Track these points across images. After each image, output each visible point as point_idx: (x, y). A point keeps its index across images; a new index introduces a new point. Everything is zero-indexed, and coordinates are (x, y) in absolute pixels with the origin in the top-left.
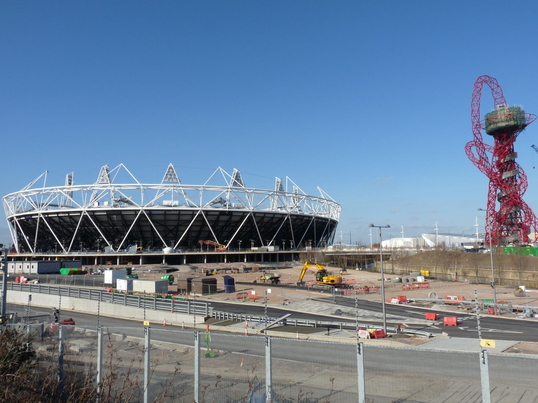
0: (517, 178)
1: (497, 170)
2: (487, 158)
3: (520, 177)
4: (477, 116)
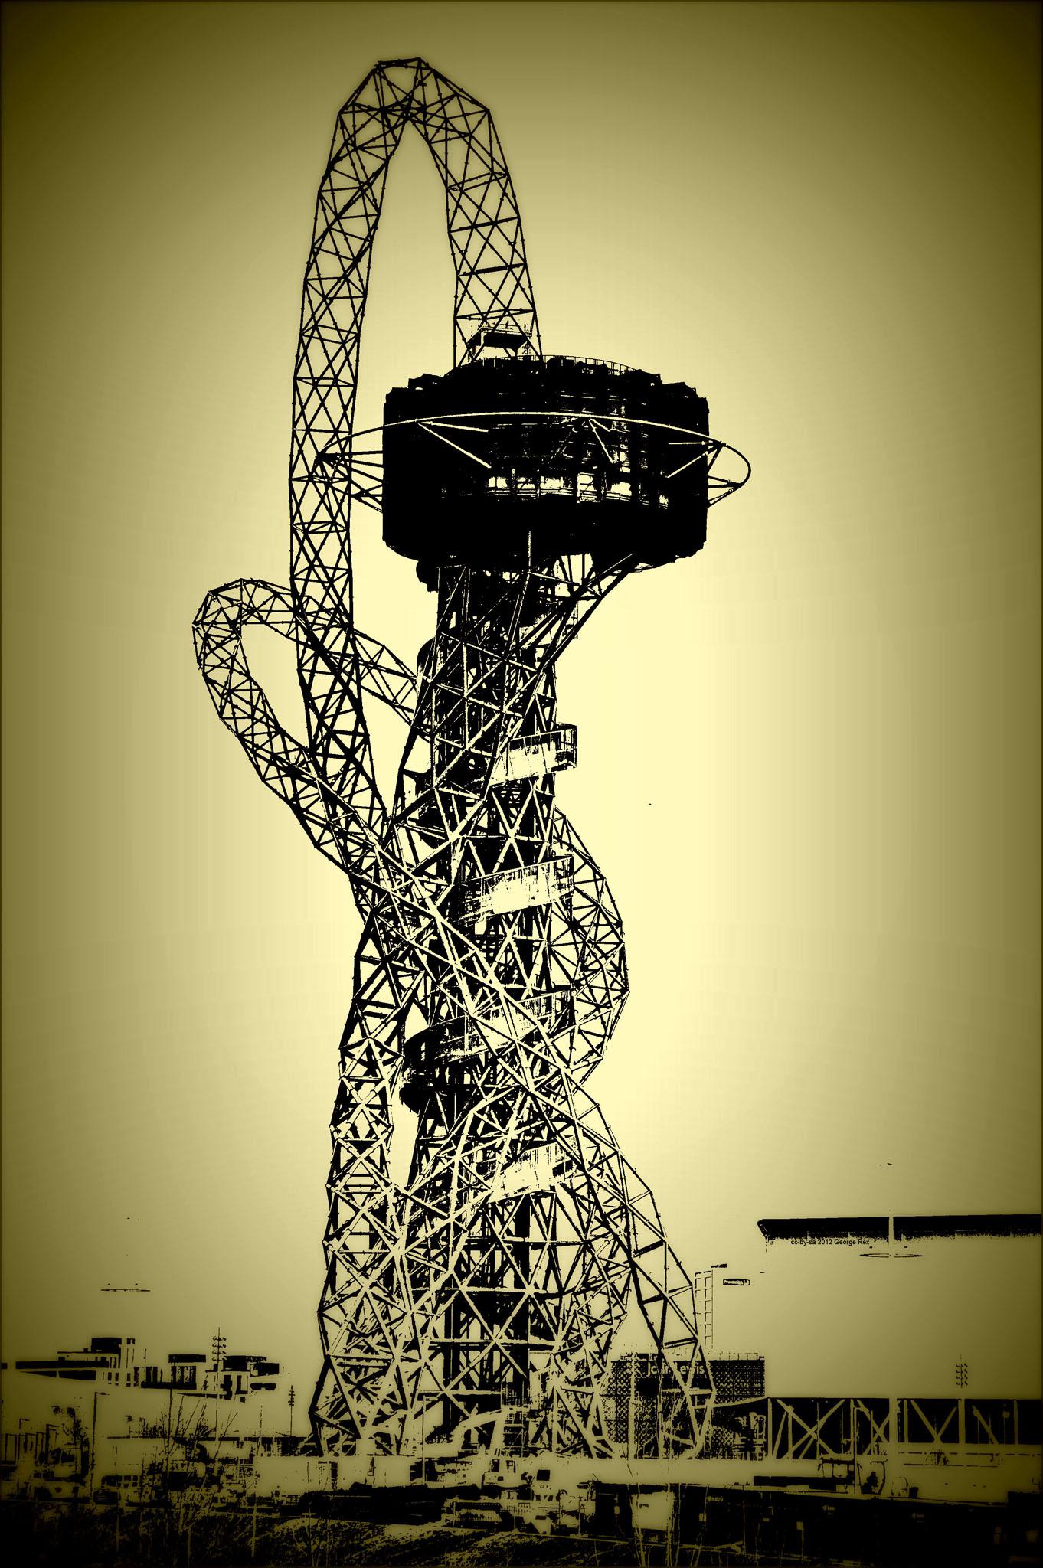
2: (366, 735)
3: (574, 925)
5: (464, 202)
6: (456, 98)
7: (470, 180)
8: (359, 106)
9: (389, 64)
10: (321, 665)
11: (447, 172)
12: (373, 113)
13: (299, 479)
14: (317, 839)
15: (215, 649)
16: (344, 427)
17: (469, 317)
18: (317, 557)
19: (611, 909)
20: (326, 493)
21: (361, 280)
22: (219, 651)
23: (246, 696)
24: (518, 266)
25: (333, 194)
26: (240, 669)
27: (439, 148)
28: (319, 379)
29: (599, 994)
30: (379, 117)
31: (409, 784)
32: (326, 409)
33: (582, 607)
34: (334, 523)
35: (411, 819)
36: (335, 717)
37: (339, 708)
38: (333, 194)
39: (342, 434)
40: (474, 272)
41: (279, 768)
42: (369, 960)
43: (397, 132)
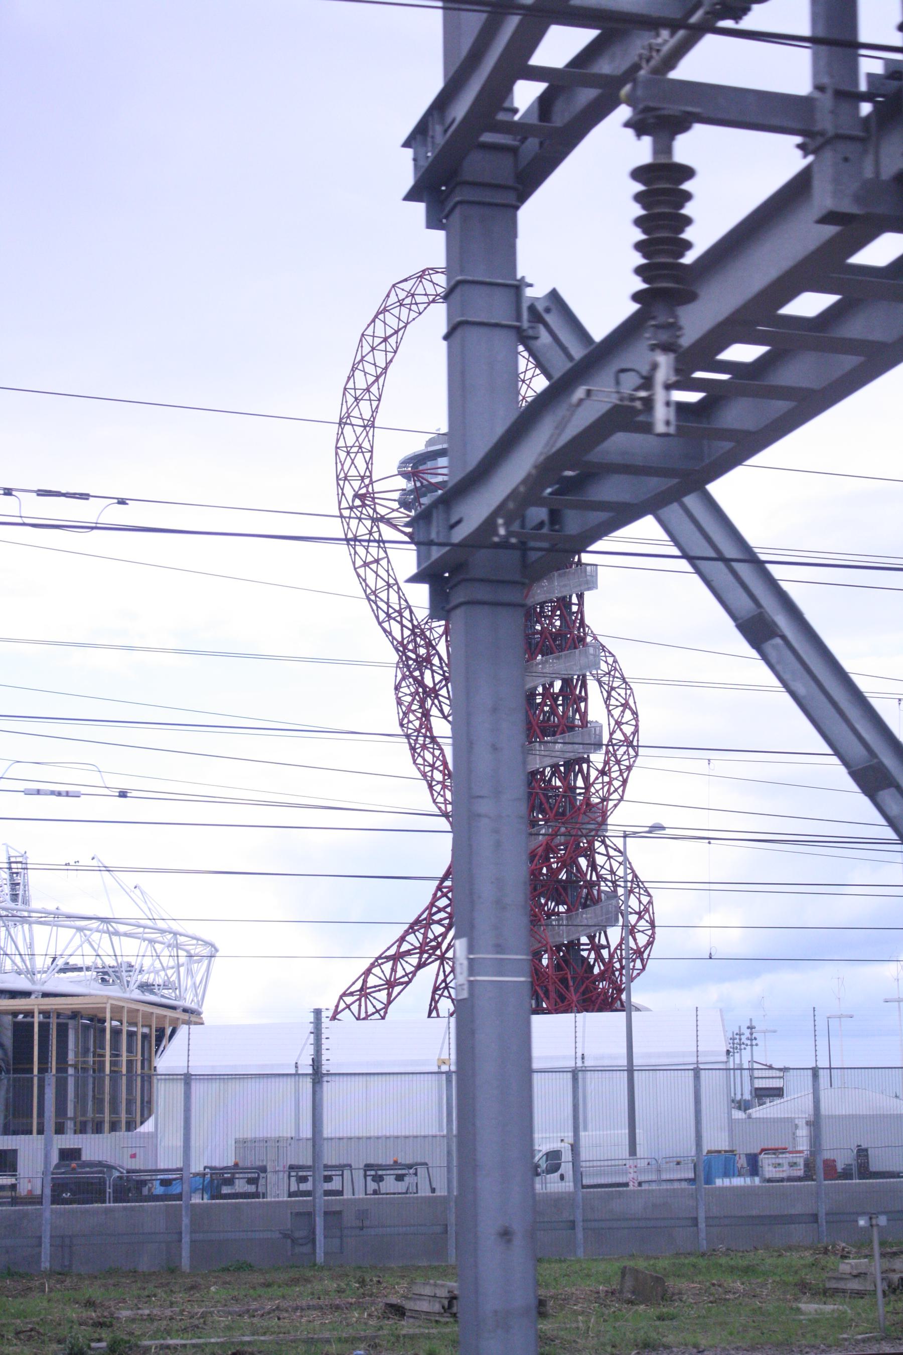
39: (367, 478)
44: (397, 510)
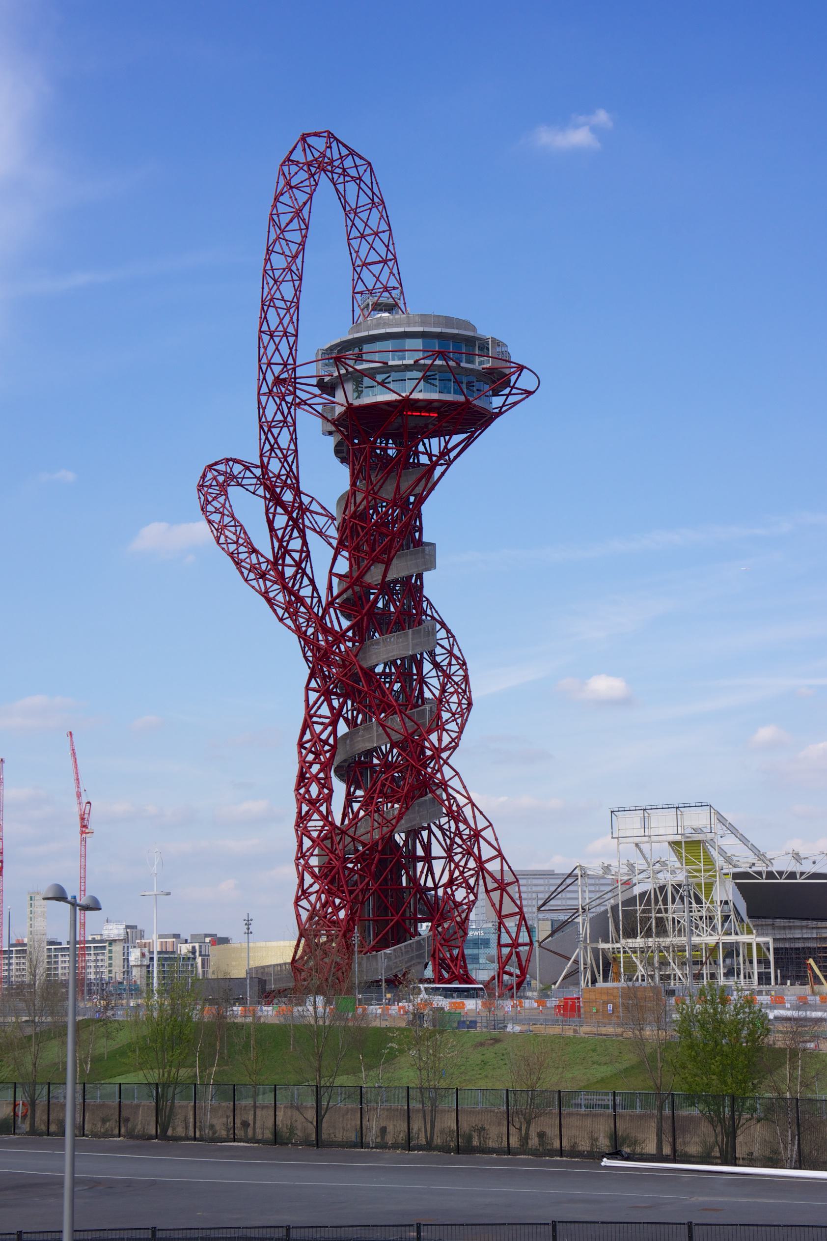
0: (427, 666)
1: (346, 624)
2: (308, 552)
3: (436, 665)
4: (286, 333)
5: (357, 221)
6: (351, 156)
7: (360, 207)
8: (292, 161)
9: (309, 135)
10: (279, 510)
11: (346, 201)
12: (301, 165)
13: (264, 394)
14: (280, 616)
15: (212, 501)
16: (291, 361)
17: (361, 293)
18: (276, 442)
19: (459, 655)
20: (281, 404)
21: (298, 269)
22: (215, 503)
23: (233, 529)
24: (390, 260)
25: (278, 216)
26: (228, 513)
27: (340, 187)
28: (274, 332)
29: (454, 707)
30: (305, 168)
31: (335, 580)
32: (279, 351)
33: (439, 470)
34: (285, 421)
35: (337, 603)
36: (288, 542)
37: (291, 536)
38: (278, 216)
40: (365, 264)
41: (256, 575)
42: (314, 690)
43: (316, 177)
44: (319, 396)
